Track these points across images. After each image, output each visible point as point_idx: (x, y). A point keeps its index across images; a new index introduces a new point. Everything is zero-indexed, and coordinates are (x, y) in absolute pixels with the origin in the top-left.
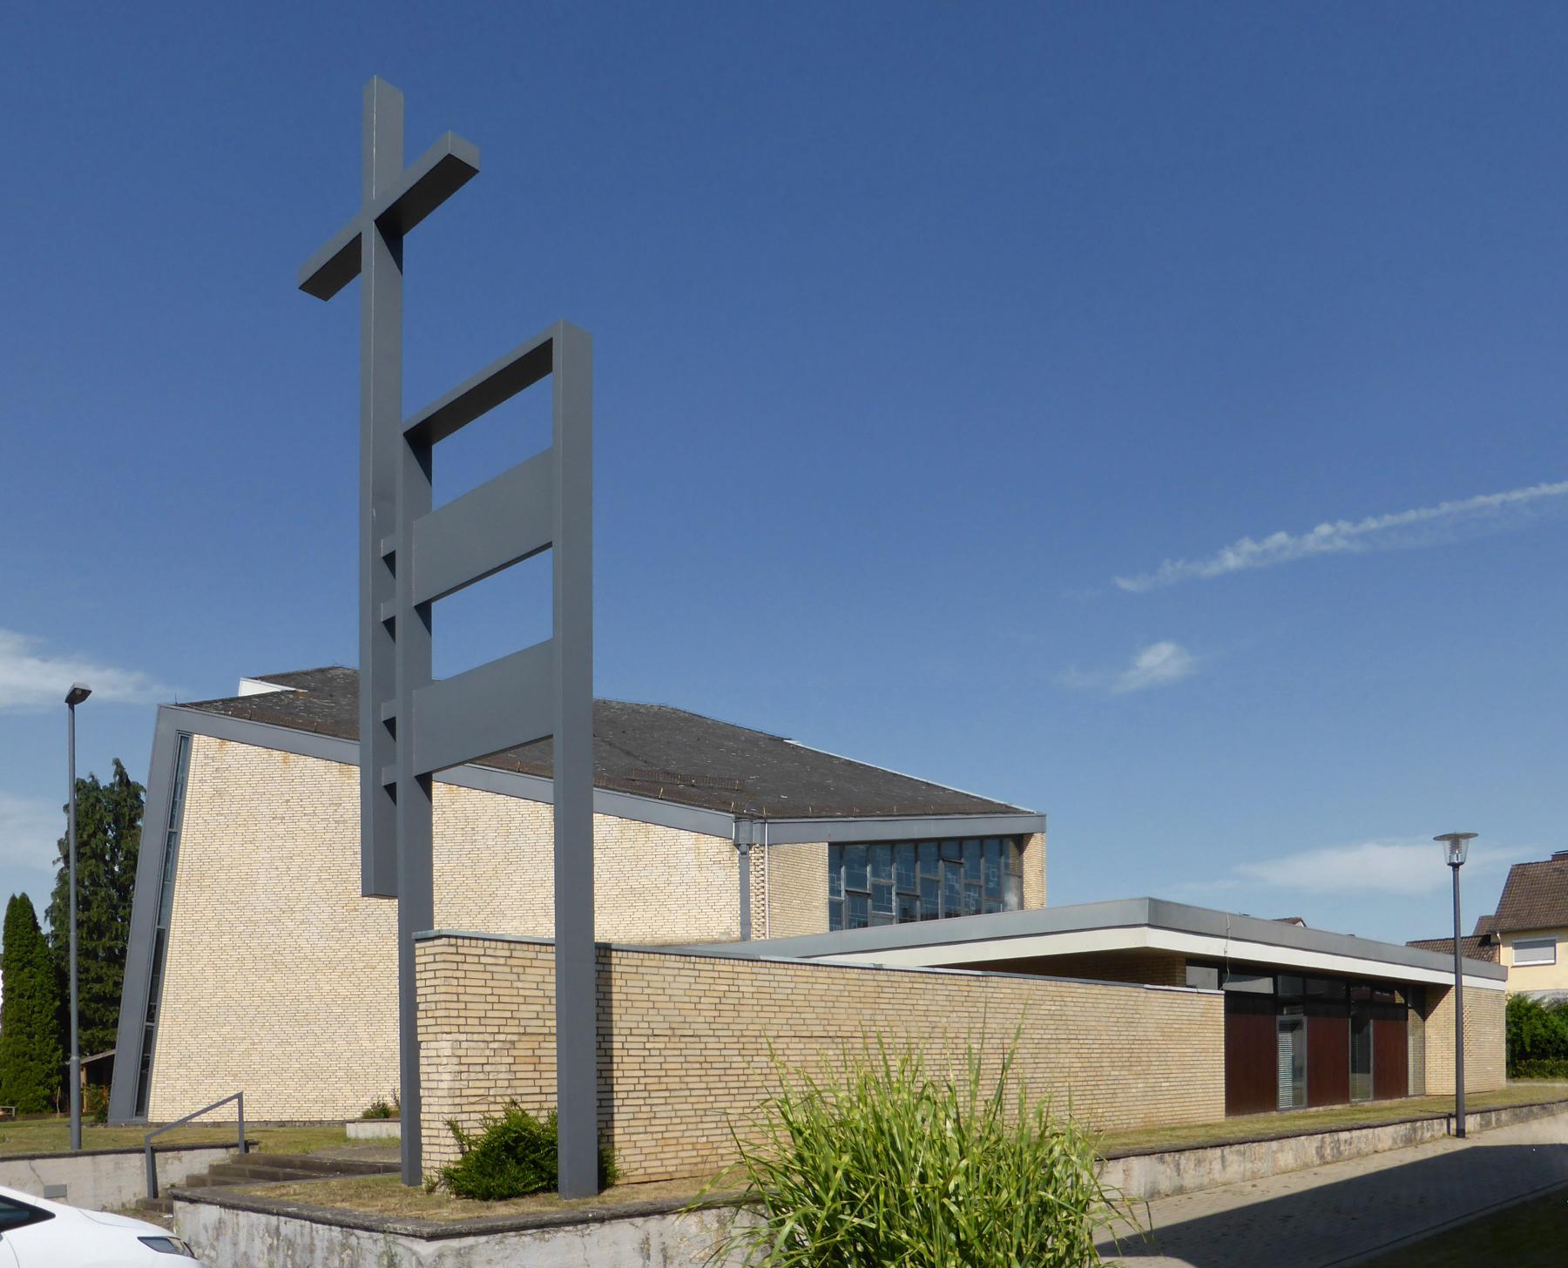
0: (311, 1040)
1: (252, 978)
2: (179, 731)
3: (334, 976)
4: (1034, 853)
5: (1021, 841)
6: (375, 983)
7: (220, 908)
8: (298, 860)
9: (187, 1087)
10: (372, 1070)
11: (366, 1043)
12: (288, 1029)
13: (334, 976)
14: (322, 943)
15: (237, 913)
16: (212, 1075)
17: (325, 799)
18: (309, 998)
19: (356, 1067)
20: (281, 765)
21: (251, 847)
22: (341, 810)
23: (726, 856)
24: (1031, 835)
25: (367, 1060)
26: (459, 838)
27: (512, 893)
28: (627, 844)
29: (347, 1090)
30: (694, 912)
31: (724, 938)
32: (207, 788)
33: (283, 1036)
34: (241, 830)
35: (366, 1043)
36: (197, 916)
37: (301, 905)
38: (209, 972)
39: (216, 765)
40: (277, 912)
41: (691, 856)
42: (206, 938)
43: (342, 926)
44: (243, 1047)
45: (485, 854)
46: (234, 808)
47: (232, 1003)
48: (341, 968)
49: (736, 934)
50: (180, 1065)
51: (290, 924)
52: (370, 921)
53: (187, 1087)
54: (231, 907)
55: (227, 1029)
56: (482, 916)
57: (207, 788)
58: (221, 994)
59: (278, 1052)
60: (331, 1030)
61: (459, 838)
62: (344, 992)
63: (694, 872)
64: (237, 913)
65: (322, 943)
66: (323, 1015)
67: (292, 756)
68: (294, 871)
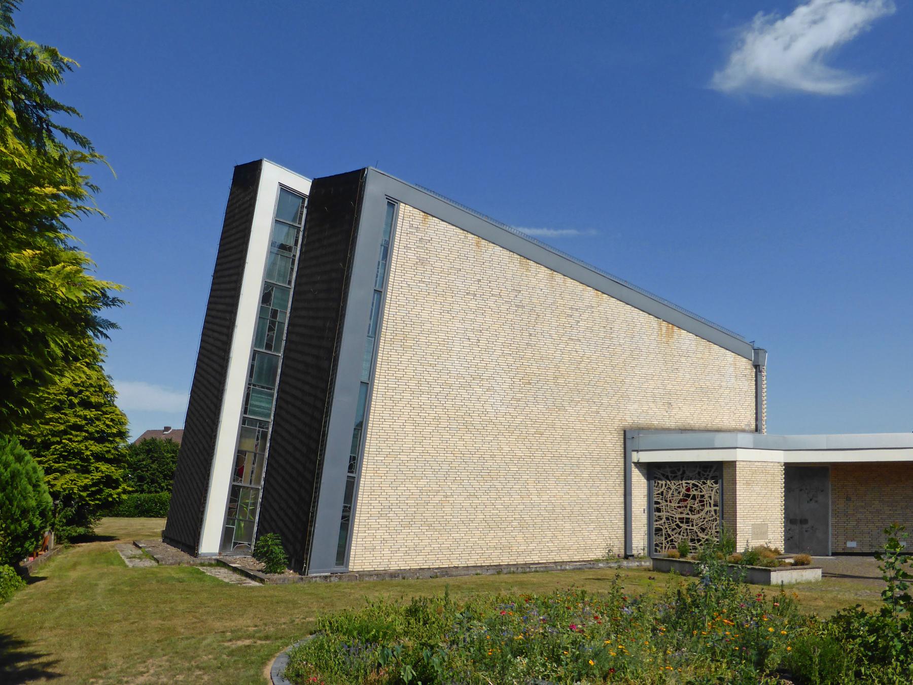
0: (493, 494)
1: (447, 436)
2: (388, 197)
3: (513, 438)
6: (543, 447)
7: (420, 368)
9: (386, 536)
10: (538, 521)
11: (535, 498)
12: (476, 484)
13: (513, 438)
14: (503, 409)
15: (435, 375)
16: (410, 526)
19: (527, 518)
21: (448, 316)
23: (747, 372)
25: (535, 512)
26: (602, 335)
27: (635, 382)
29: (520, 538)
31: (747, 428)
32: (411, 254)
33: (471, 490)
34: (440, 299)
35: (535, 498)
38: (409, 428)
39: (420, 235)
40: (469, 379)
41: (732, 369)
42: (407, 395)
43: (519, 396)
44: (438, 498)
45: (619, 349)
46: (435, 278)
47: (428, 458)
49: (753, 427)
50: (381, 516)
51: (479, 391)
52: (540, 393)
53: (386, 536)
54: (430, 369)
55: (423, 482)
56: (615, 398)
57: (411, 254)
58: (419, 449)
59: (466, 504)
60: (509, 485)
61: (602, 335)
63: (733, 380)
65: (503, 409)
66: (502, 473)
67: (483, 242)
68: (483, 343)
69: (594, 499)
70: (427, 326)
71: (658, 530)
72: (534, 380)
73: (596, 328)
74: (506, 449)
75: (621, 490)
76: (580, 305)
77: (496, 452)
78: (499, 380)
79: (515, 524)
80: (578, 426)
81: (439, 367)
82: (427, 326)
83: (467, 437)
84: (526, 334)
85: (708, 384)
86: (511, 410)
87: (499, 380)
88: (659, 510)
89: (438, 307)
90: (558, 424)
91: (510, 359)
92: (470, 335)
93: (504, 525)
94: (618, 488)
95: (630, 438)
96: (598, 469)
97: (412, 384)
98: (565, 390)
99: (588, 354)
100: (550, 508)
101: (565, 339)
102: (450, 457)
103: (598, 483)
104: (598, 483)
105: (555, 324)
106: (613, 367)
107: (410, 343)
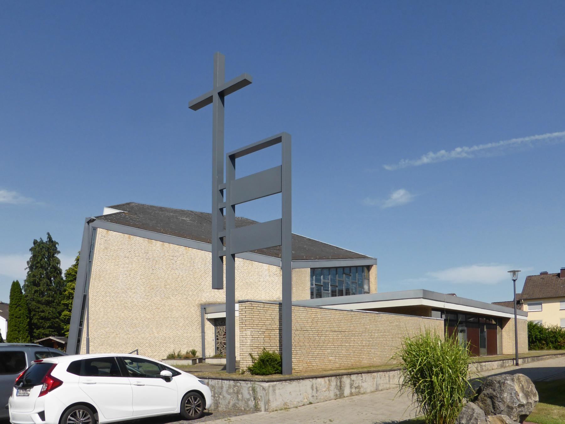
0: (137, 333)
3: (145, 311)
4: (373, 271)
5: (369, 267)
7: (106, 287)
8: (133, 272)
10: (158, 344)
12: (129, 330)
13: (145, 311)
14: (141, 300)
15: (112, 289)
16: (102, 345)
17: (143, 251)
18: (137, 319)
19: (152, 342)
20: (128, 239)
22: (148, 255)
23: (278, 272)
24: (372, 266)
26: (189, 265)
27: (206, 284)
28: (246, 268)
29: (149, 350)
30: (268, 291)
32: (102, 246)
33: (127, 332)
36: (98, 290)
37: (134, 287)
38: (102, 310)
39: (105, 239)
40: (126, 289)
41: (267, 272)
42: (101, 298)
43: (148, 294)
44: (113, 335)
48: (147, 308)
51: (131, 294)
55: (107, 330)
56: (196, 291)
57: (102, 246)
58: (106, 317)
60: (144, 330)
62: (149, 317)
63: (268, 277)
64: (112, 289)
65: (141, 300)
66: (141, 325)
67: (132, 236)
68: (132, 275)
69: (185, 335)
70: (109, 271)
71: (218, 348)
72: (155, 287)
73: (185, 263)
74: (142, 315)
75: (200, 331)
76: (177, 254)
77: (138, 317)
78: (139, 288)
79: (147, 345)
80: (177, 304)
81: (114, 286)
82: (109, 271)
83: (125, 312)
84: (151, 269)
85: (251, 280)
86: (145, 300)
87: (139, 288)
88: (218, 339)
89: (113, 264)
90: (167, 304)
91: (144, 280)
92: (126, 273)
93: (142, 345)
94: (198, 330)
95: (204, 308)
96: (187, 322)
97: (103, 293)
98: (170, 290)
99: (181, 274)
100: (163, 338)
101: (170, 269)
102: (118, 320)
103: (187, 328)
104: (187, 328)
105: (164, 264)
106: (195, 278)
107: (102, 279)
